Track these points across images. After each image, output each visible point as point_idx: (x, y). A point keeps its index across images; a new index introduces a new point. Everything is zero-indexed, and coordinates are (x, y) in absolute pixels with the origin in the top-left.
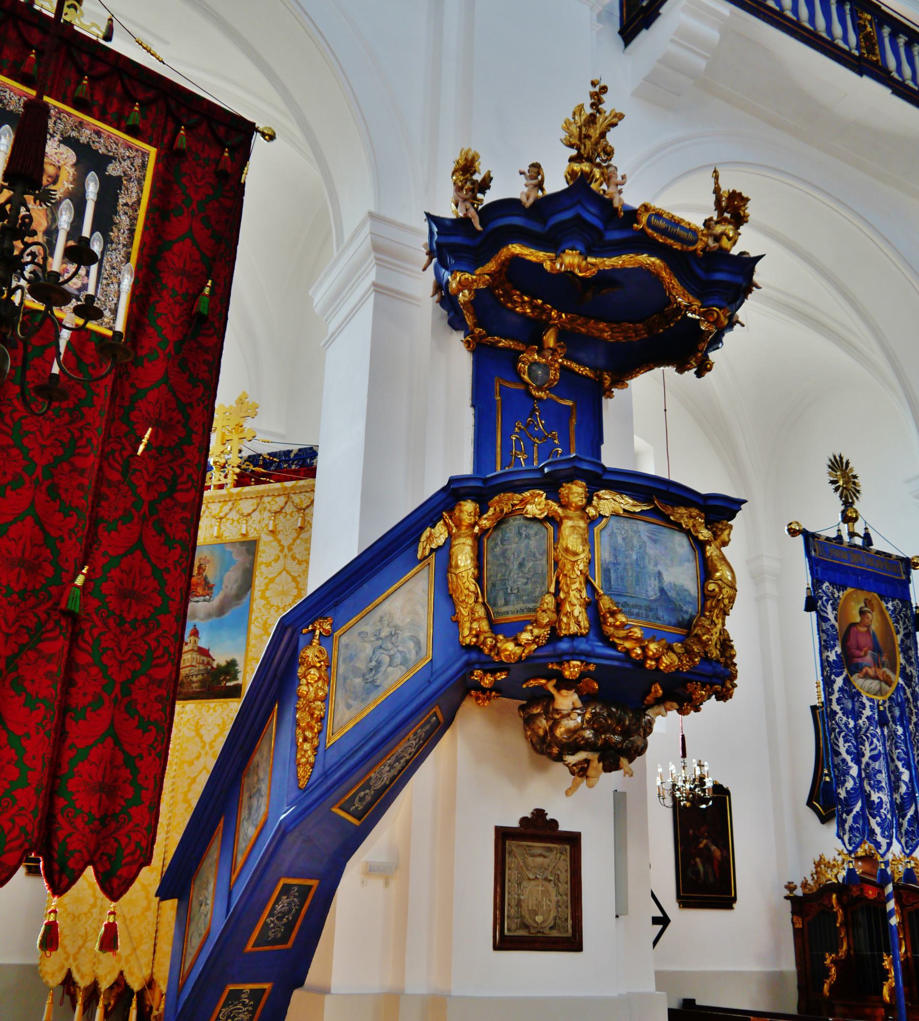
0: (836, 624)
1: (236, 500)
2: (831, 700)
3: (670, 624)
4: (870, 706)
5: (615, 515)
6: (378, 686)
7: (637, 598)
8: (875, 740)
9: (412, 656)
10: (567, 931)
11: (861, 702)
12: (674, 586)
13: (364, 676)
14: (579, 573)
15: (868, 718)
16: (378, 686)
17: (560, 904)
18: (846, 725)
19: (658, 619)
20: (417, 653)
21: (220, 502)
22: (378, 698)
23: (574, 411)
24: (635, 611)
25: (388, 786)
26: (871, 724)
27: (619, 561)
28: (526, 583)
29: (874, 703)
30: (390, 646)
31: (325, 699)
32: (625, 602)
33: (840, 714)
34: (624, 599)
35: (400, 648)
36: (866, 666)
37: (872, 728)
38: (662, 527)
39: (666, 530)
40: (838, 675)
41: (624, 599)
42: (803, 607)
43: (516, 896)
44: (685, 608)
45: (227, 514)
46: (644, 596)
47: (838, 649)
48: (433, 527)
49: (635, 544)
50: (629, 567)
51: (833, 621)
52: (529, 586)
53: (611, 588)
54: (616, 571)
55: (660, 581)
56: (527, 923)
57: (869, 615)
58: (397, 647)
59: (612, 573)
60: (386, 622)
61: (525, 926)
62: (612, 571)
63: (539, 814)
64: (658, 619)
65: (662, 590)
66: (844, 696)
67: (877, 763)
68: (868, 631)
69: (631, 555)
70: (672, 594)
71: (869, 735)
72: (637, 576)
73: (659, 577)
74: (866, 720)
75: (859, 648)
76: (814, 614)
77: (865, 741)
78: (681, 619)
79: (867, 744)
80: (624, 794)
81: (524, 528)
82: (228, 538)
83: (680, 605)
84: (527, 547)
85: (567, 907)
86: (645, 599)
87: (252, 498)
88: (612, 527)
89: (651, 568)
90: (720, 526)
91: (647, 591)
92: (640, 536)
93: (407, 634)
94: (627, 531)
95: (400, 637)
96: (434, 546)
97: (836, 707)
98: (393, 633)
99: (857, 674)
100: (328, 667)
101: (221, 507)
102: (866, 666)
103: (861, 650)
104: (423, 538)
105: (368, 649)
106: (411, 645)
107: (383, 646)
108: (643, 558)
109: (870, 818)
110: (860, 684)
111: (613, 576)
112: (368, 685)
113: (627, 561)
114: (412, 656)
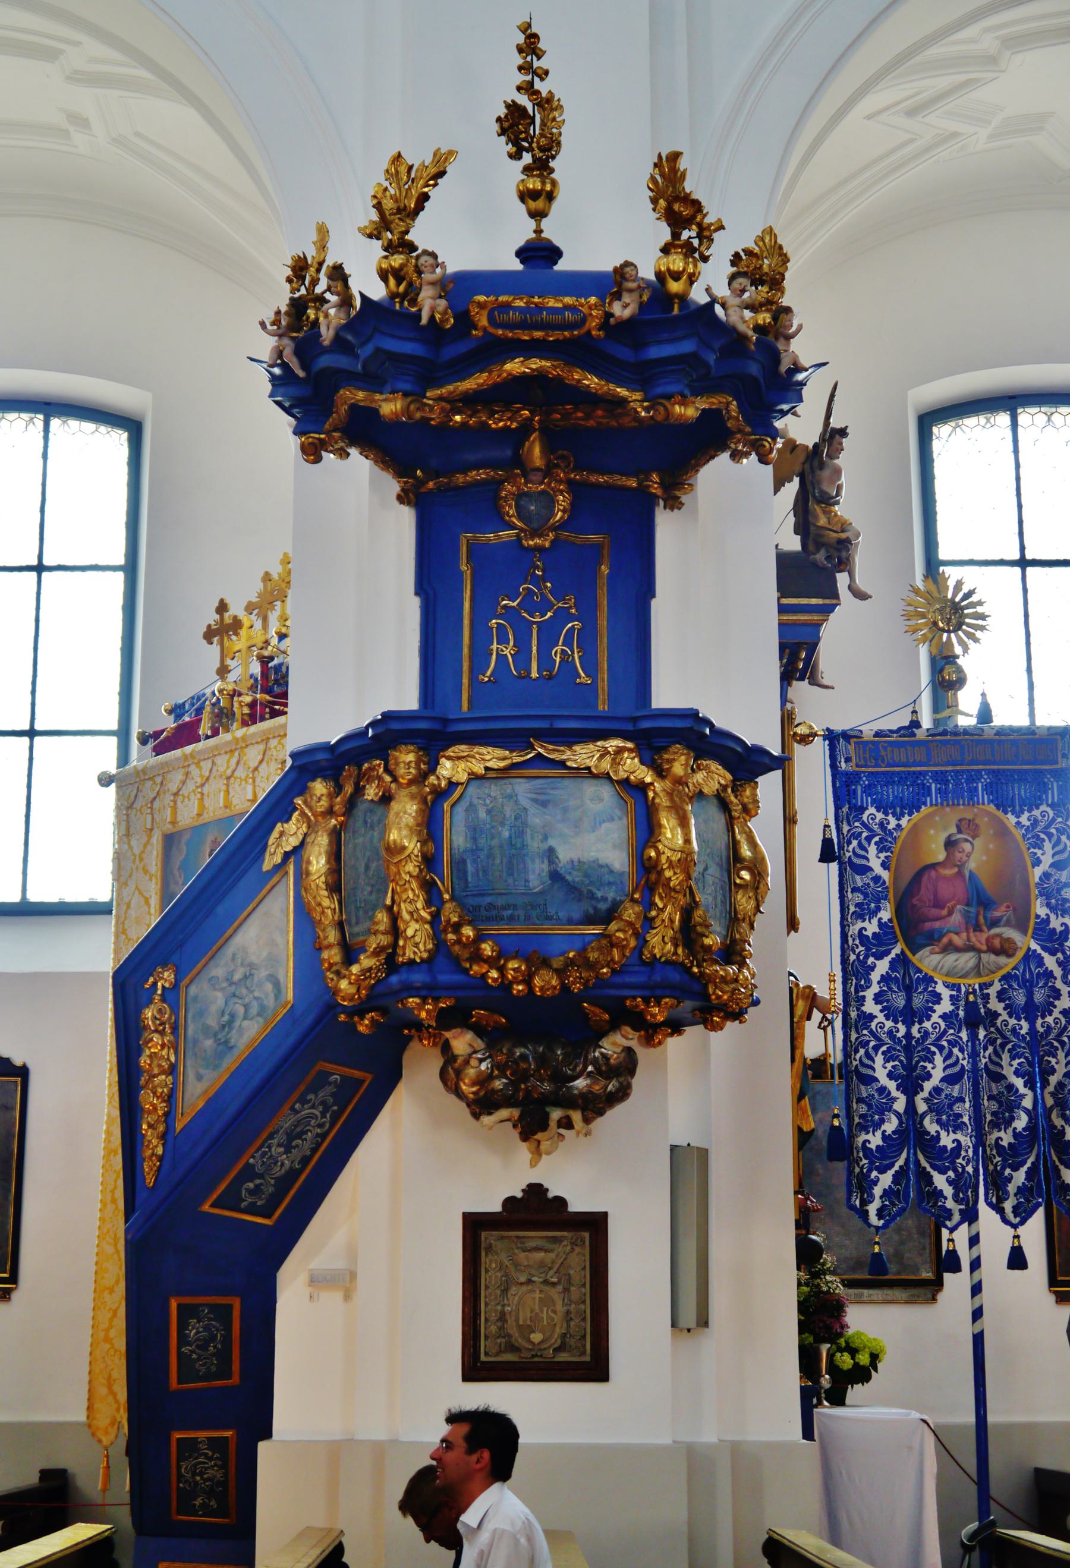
0: (885, 875)
1: (242, 747)
2: (864, 997)
3: (570, 922)
4: (951, 996)
6: (232, 1048)
7: (511, 894)
8: (956, 1051)
9: (270, 1002)
10: (584, 1353)
11: (934, 991)
12: (576, 865)
13: (215, 1035)
14: (407, 878)
15: (944, 1017)
16: (232, 1048)
17: (572, 1316)
18: (890, 1034)
19: (549, 918)
21: (226, 753)
22: (230, 1063)
23: (605, 552)
24: (507, 913)
25: (299, 1172)
26: (949, 1026)
27: (480, 845)
28: (371, 893)
29: (959, 990)
30: (244, 991)
31: (172, 1070)
33: (881, 1017)
34: (489, 899)
35: (256, 994)
36: (949, 932)
37: (951, 1031)
38: (559, 779)
39: (566, 782)
40: (879, 956)
41: (489, 899)
43: (499, 1308)
44: (599, 894)
47: (885, 915)
49: (507, 816)
50: (497, 851)
51: (878, 870)
52: (373, 897)
53: (467, 887)
54: (474, 861)
55: (551, 862)
56: (516, 1344)
57: (967, 847)
58: (252, 992)
59: (469, 865)
60: (239, 961)
61: (513, 1348)
62: (469, 862)
63: (535, 1190)
64: (549, 918)
65: (555, 876)
66: (890, 989)
67: (957, 1087)
68: (960, 873)
69: (500, 833)
70: (574, 877)
71: (945, 1043)
72: (510, 864)
73: (549, 857)
74: (940, 1021)
75: (938, 904)
76: (834, 866)
78: (591, 911)
79: (938, 1059)
80: (703, 1154)
81: (369, 814)
83: (590, 892)
84: (371, 841)
85: (584, 1319)
86: (523, 894)
88: (471, 797)
89: (534, 844)
90: (666, 756)
91: (527, 881)
92: (516, 802)
93: (263, 973)
94: (495, 798)
95: (256, 979)
96: (288, 849)
97: (870, 1007)
98: (248, 974)
99: (929, 948)
100: (175, 1029)
101: (228, 761)
102: (949, 932)
103: (943, 908)
104: (271, 840)
105: (219, 999)
106: (269, 987)
108: (521, 834)
109: (1062, 1167)
110: (934, 963)
111: (470, 868)
112: (221, 1048)
113: (495, 842)
114: (270, 1002)
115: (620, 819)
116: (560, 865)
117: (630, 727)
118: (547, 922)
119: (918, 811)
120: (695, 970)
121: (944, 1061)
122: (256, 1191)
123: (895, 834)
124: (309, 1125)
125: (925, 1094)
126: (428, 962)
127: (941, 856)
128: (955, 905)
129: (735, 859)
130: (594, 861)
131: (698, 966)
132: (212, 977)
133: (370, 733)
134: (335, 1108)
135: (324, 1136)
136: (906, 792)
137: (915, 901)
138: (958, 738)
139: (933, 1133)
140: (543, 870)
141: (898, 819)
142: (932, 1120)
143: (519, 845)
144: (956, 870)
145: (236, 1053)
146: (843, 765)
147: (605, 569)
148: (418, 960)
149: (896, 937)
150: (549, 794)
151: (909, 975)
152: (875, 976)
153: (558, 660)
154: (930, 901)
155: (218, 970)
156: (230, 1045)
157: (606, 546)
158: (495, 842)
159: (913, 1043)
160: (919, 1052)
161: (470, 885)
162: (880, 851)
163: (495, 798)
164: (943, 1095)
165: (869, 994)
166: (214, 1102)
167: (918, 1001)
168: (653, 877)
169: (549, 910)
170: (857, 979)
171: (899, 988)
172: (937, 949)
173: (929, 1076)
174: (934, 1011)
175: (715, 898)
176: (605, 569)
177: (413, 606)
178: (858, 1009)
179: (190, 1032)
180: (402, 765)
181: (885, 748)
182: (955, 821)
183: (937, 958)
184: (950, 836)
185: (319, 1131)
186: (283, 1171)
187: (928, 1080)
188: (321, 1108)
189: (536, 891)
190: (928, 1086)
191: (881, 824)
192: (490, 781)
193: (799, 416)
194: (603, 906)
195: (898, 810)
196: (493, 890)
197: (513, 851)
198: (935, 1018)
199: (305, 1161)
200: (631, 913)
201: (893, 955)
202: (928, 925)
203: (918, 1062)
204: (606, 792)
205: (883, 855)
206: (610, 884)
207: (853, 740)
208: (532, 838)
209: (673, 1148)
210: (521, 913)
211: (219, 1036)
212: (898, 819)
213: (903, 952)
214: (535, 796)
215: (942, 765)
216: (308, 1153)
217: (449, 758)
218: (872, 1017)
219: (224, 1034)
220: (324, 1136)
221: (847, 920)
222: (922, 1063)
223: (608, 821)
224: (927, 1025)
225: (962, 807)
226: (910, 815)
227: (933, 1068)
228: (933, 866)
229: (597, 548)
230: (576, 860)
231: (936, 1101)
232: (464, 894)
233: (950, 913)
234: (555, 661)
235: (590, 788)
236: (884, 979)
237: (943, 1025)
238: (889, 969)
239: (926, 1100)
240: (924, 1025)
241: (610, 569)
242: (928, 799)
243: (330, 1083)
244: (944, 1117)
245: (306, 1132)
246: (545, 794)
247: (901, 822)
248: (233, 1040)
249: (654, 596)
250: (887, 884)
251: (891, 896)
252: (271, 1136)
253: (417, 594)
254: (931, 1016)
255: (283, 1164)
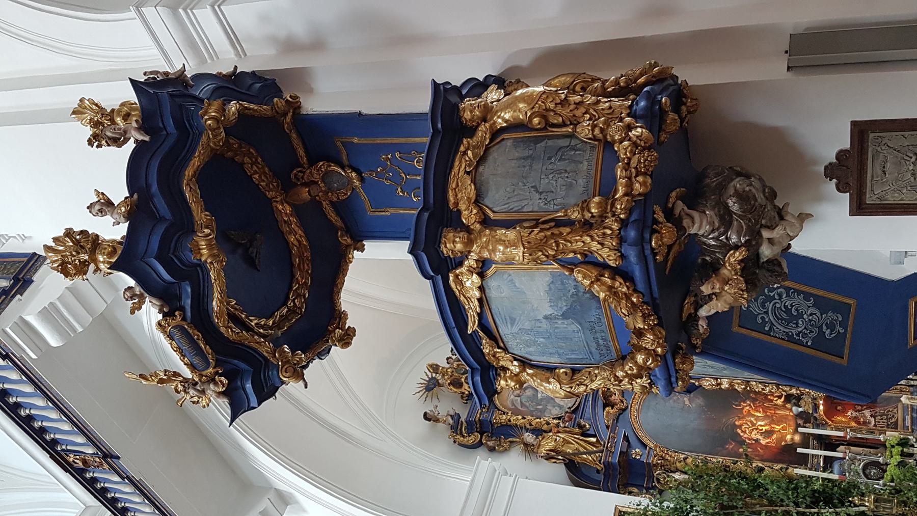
5: (506, 350)
12: (553, 302)
24: (601, 342)
34: (593, 350)
39: (493, 307)
54: (568, 355)
65: (565, 316)
70: (564, 306)
118: (602, 321)
122: (831, 327)
175: (560, 172)
186: (816, 312)
192: (506, 343)
199: (807, 296)
214: (509, 326)
245: (785, 307)
252: (791, 339)
255: (811, 315)
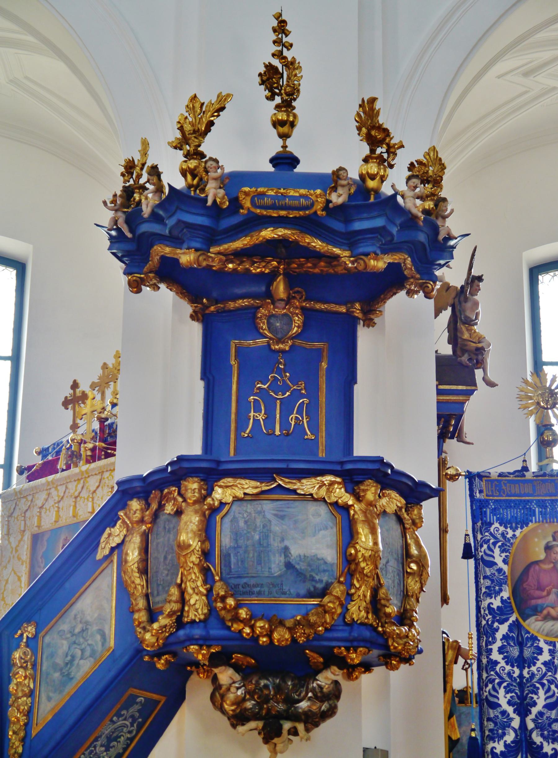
0: (505, 568)
1: (85, 477)
2: (491, 649)
3: (298, 596)
4: (550, 650)
8: (553, 687)
9: (99, 648)
12: (303, 558)
13: (61, 670)
14: (191, 565)
15: (545, 664)
16: (72, 678)
18: (509, 674)
19: (284, 593)
20: (103, 645)
22: (71, 689)
23: (325, 354)
24: (257, 590)
27: (240, 544)
28: (167, 575)
30: (81, 640)
31: (31, 694)
32: (245, 583)
33: (503, 663)
34: (245, 580)
35: (90, 642)
36: (548, 606)
37: (550, 674)
39: (297, 503)
40: (502, 622)
41: (245, 580)
42: (461, 555)
44: (317, 578)
45: (80, 493)
46: (266, 574)
47: (506, 594)
48: (114, 526)
49: (258, 524)
50: (250, 548)
51: (501, 565)
52: (169, 578)
53: (231, 572)
54: (236, 555)
55: (286, 556)
58: (87, 641)
60: (79, 619)
62: (232, 555)
64: (284, 593)
65: (289, 566)
66: (509, 644)
69: (253, 537)
70: (301, 566)
71: (545, 682)
72: (259, 555)
73: (285, 552)
74: (542, 666)
75: (540, 588)
76: (472, 561)
77: (538, 688)
78: (312, 589)
79: (541, 692)
81: (167, 523)
82: (81, 517)
83: (311, 576)
84: (169, 540)
86: (268, 577)
87: (96, 474)
88: (234, 512)
89: (275, 544)
90: (362, 487)
91: (270, 568)
92: (264, 517)
93: (95, 628)
94: (250, 513)
95: (89, 631)
96: (114, 545)
98: (84, 628)
99: (534, 617)
100: (34, 666)
102: (548, 606)
103: (543, 590)
104: (103, 539)
105: (65, 644)
106: (98, 637)
107: (77, 641)
108: (267, 537)
110: (538, 627)
111: (233, 560)
112: (64, 678)
113: (249, 543)
114: (99, 648)
115: (332, 528)
116: (292, 558)
117: (338, 468)
118: (283, 596)
119: (527, 526)
120: (380, 629)
121: (546, 693)
123: (512, 541)
124: (122, 731)
125: (532, 716)
126: (204, 621)
127: (542, 556)
128: (552, 589)
129: (407, 555)
130: (314, 556)
131: (383, 626)
132: (61, 631)
133: (169, 469)
134: (140, 720)
135: (131, 740)
136: (519, 513)
137: (525, 585)
138: (553, 478)
139: (538, 743)
140: (280, 561)
141: (514, 531)
142: (537, 734)
143: (265, 545)
144: (552, 565)
145: (74, 682)
146: (478, 495)
147: (324, 365)
148: (197, 620)
149: (513, 609)
150: (285, 511)
151: (522, 635)
152: (499, 635)
153: (293, 423)
154: (535, 585)
155: (64, 626)
156: (72, 676)
157: (325, 350)
158: (249, 543)
159: (524, 681)
160: (528, 687)
161: (233, 570)
162: (502, 552)
163: (250, 513)
164: (545, 717)
165: (495, 647)
166: (58, 716)
167: (527, 653)
168: (353, 567)
169: (284, 588)
170: (486, 637)
171: (514, 643)
172: (540, 618)
173: (535, 704)
174: (538, 660)
175: (393, 581)
176: (324, 365)
177: (200, 386)
178: (488, 657)
179: (44, 668)
180: (189, 491)
181: (505, 484)
182: (551, 534)
183: (539, 624)
184: (548, 543)
185: (129, 736)
187: (535, 706)
188: (130, 720)
189: (276, 575)
190: (535, 711)
191: (503, 535)
193: (451, 268)
194: (320, 586)
195: (514, 525)
196: (248, 574)
197: (261, 549)
198: (539, 664)
200: (338, 590)
201: (510, 621)
202: (533, 602)
203: (528, 694)
204: (323, 510)
205: (504, 555)
206: (325, 571)
207: (484, 479)
208: (274, 540)
209: (365, 750)
210: (266, 589)
211: (64, 671)
212: (514, 531)
213: (517, 619)
214: (276, 512)
215: (543, 496)
216: (121, 751)
217: (220, 487)
218: (496, 663)
219: (67, 669)
220: (131, 740)
221: (480, 597)
222: (530, 695)
223: (324, 530)
224: (534, 669)
225: (555, 523)
226: (522, 528)
227: (538, 699)
228: (537, 563)
229: (319, 351)
230: (302, 554)
231: (540, 721)
232: (229, 576)
233: (549, 594)
234: (291, 424)
235: (312, 507)
236: (505, 637)
237: (544, 669)
238: (508, 631)
239: (533, 720)
240: (531, 669)
241: (328, 364)
242: (534, 518)
243: (137, 703)
244: (546, 732)
245: (120, 737)
246: (282, 511)
247: (516, 533)
248: (73, 673)
249: (356, 383)
250: (507, 574)
251: (509, 582)
252: (96, 740)
253: (202, 379)
254: (536, 663)
